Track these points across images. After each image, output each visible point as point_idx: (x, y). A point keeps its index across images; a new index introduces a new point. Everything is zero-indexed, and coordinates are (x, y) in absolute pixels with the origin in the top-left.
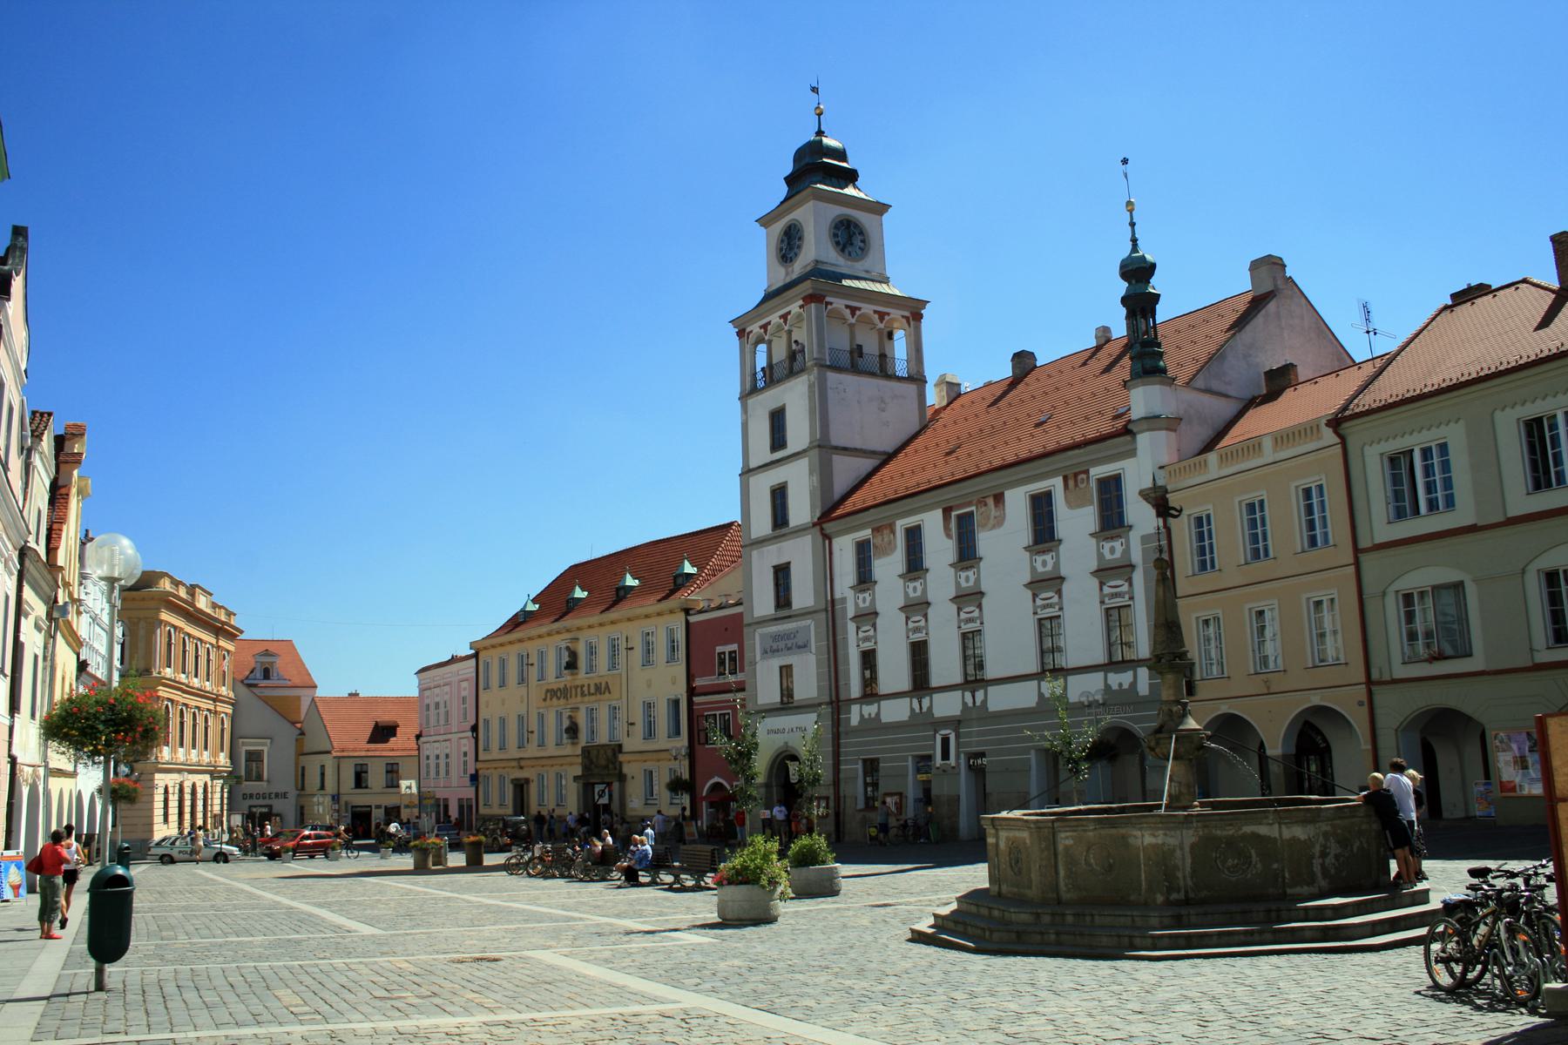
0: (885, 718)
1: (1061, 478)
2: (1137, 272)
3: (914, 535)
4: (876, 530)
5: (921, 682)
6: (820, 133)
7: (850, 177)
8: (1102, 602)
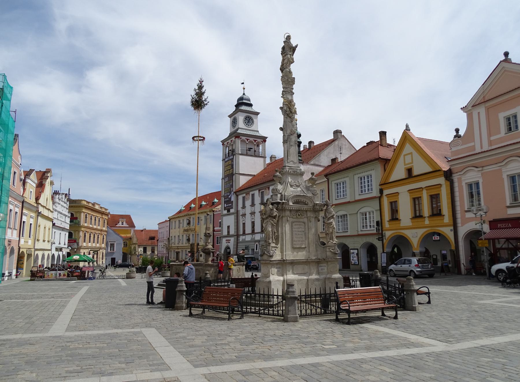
0: (247, 240)
3: (253, 195)
4: (246, 194)
5: (253, 232)
6: (244, 94)
7: (250, 105)
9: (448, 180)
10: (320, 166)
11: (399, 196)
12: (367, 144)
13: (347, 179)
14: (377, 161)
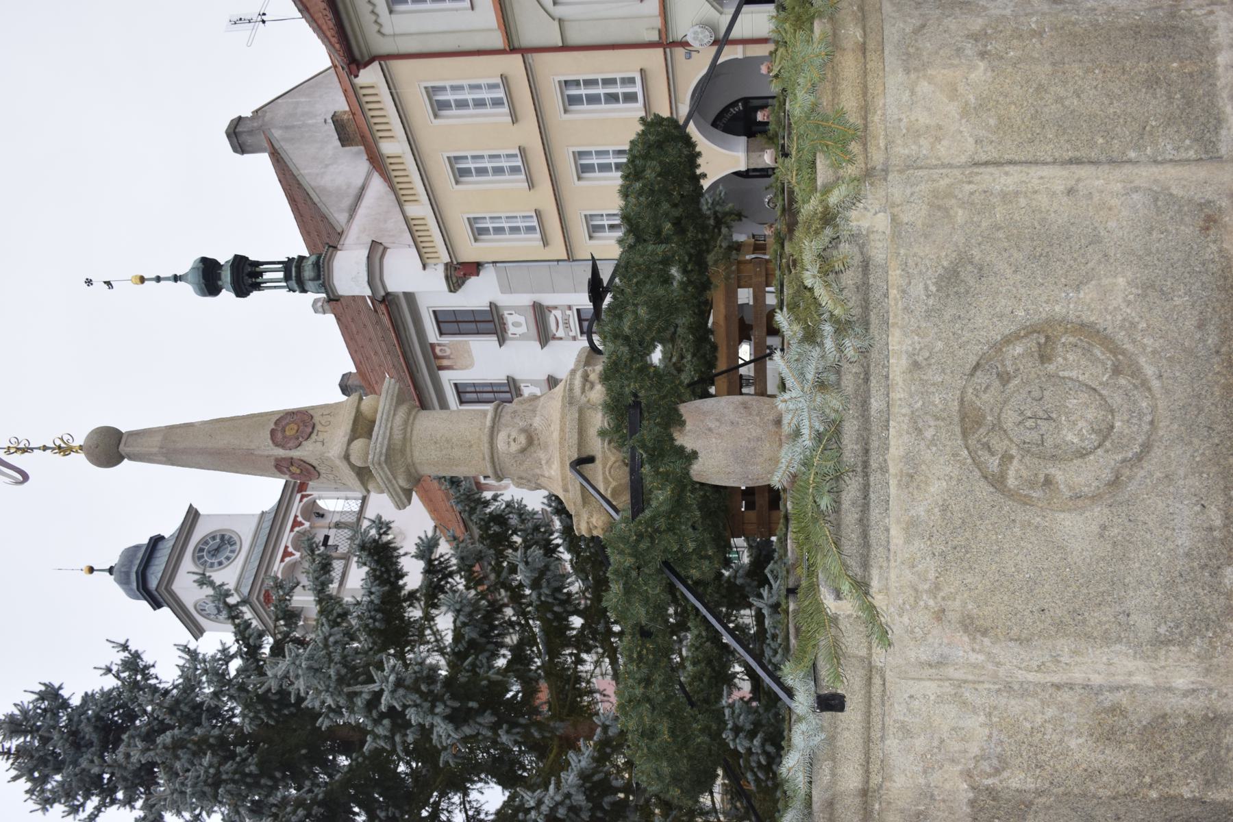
1: (441, 373)
2: (209, 277)
6: (110, 570)
7: (156, 541)
8: (574, 338)
10: (363, 188)
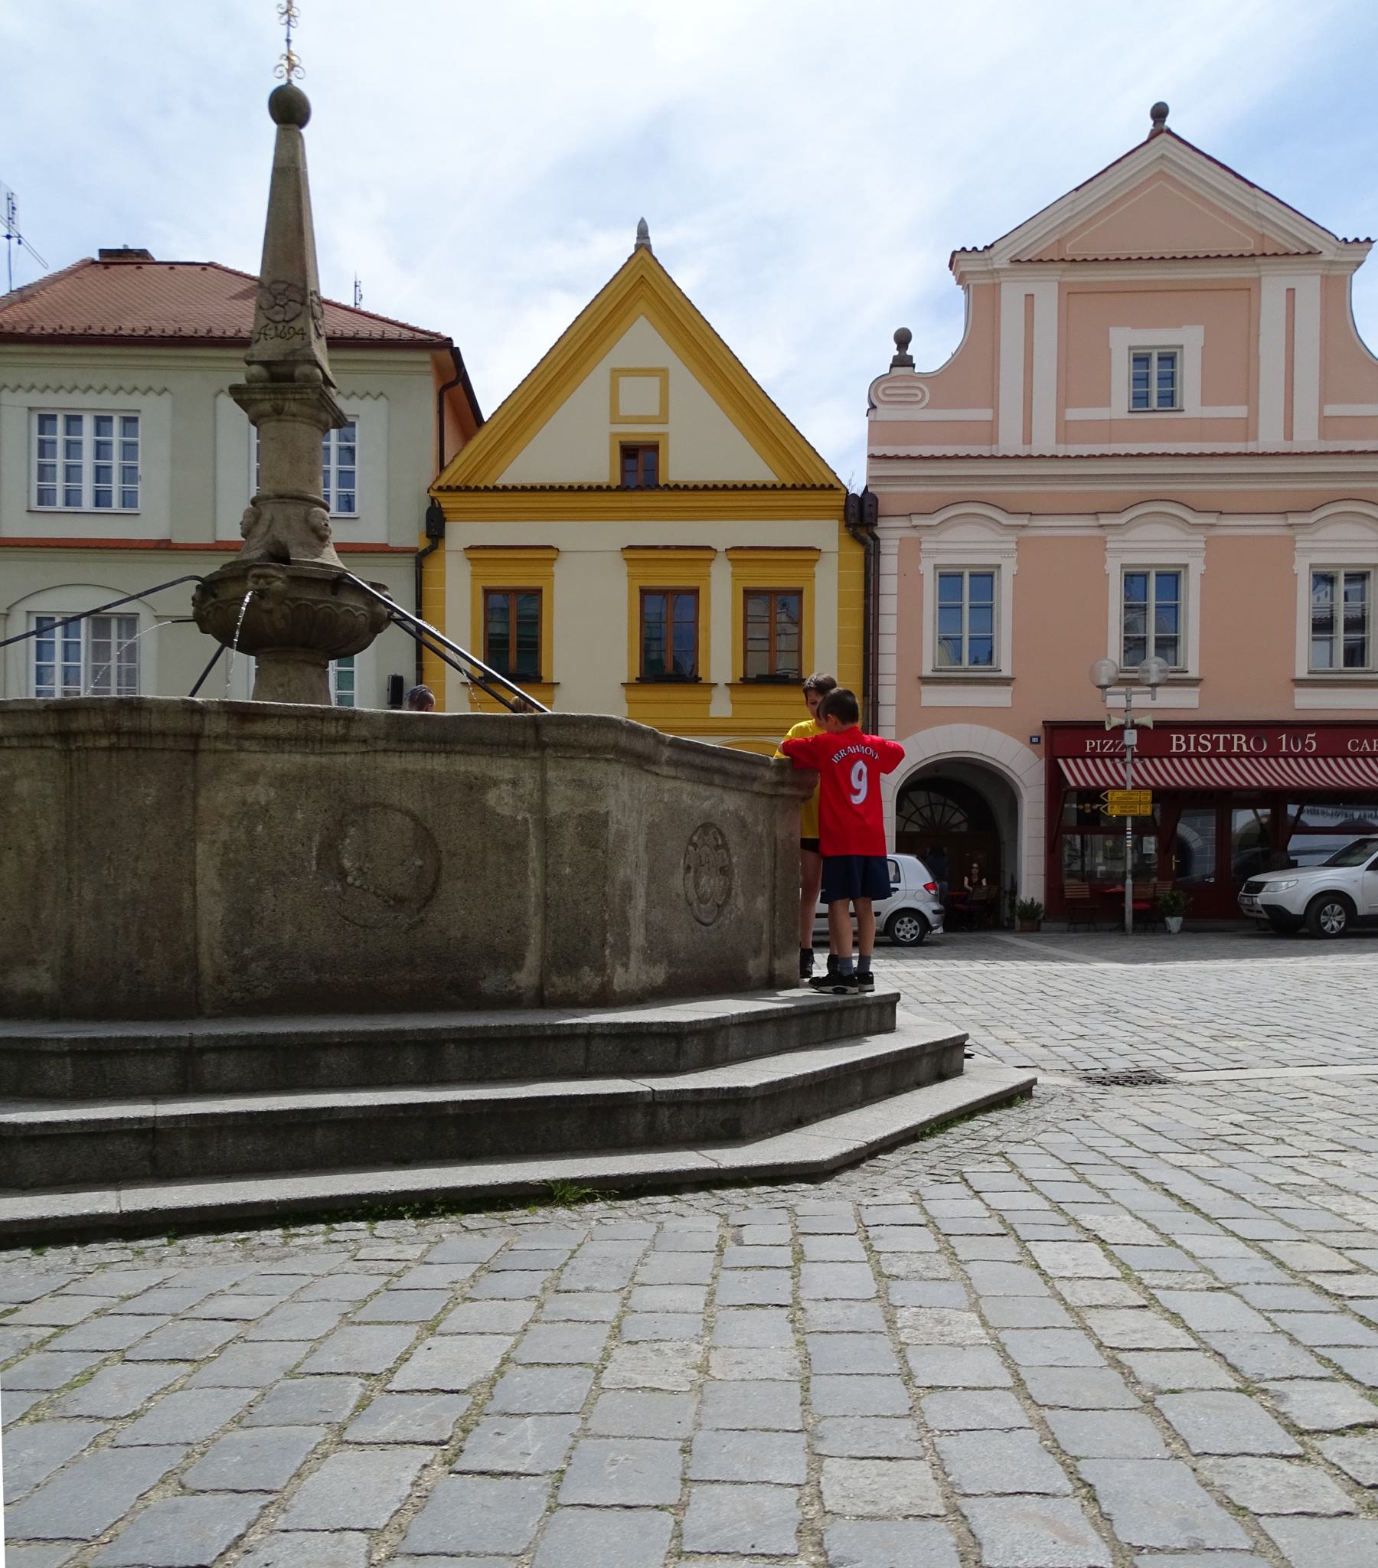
9: (862, 542)
11: (557, 569)
12: (102, 252)
13: (154, 412)
14: (425, 356)
